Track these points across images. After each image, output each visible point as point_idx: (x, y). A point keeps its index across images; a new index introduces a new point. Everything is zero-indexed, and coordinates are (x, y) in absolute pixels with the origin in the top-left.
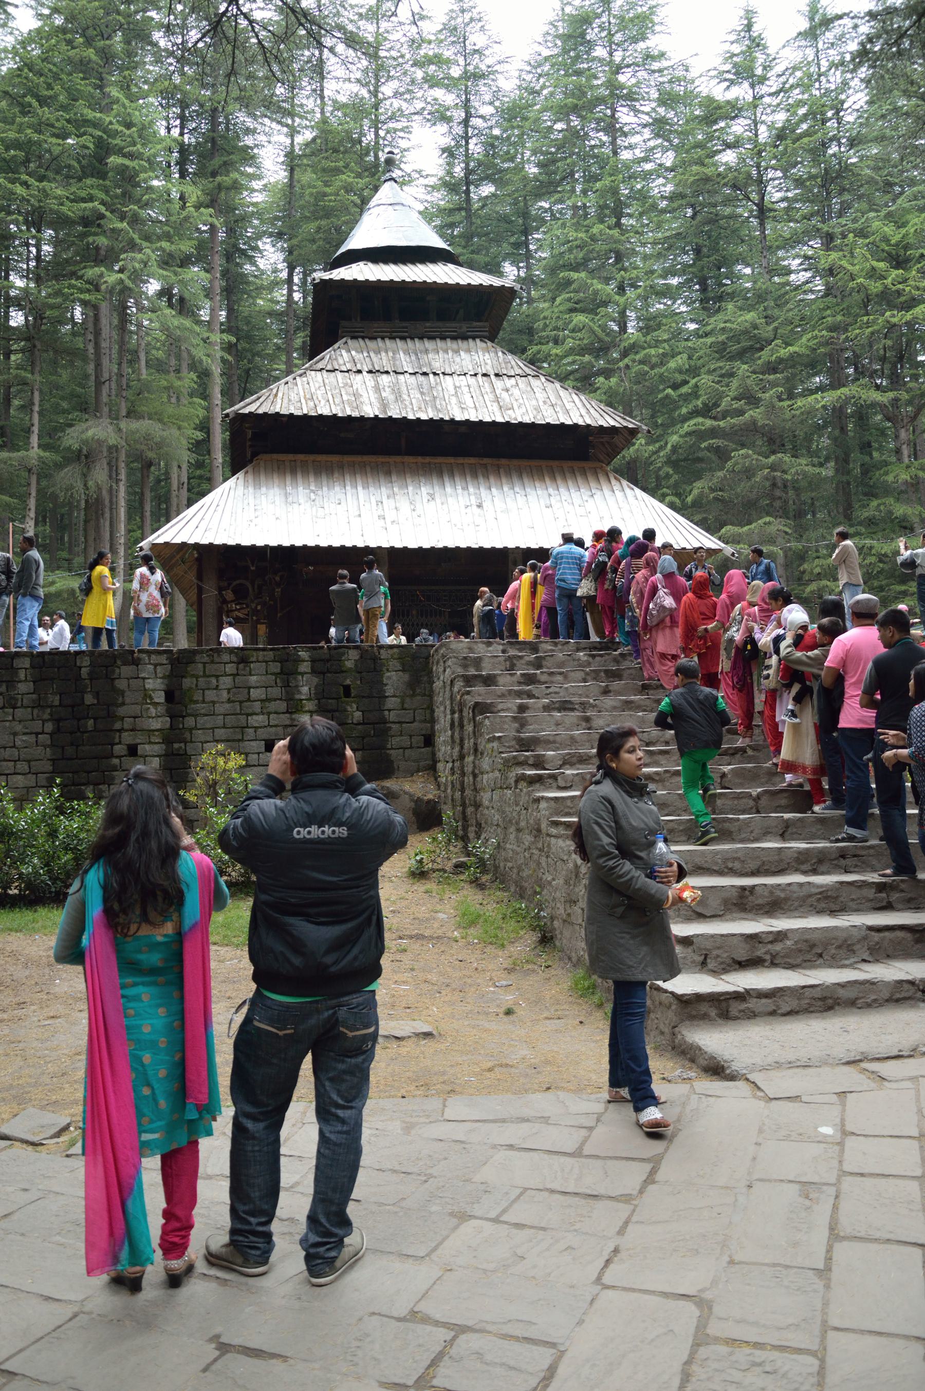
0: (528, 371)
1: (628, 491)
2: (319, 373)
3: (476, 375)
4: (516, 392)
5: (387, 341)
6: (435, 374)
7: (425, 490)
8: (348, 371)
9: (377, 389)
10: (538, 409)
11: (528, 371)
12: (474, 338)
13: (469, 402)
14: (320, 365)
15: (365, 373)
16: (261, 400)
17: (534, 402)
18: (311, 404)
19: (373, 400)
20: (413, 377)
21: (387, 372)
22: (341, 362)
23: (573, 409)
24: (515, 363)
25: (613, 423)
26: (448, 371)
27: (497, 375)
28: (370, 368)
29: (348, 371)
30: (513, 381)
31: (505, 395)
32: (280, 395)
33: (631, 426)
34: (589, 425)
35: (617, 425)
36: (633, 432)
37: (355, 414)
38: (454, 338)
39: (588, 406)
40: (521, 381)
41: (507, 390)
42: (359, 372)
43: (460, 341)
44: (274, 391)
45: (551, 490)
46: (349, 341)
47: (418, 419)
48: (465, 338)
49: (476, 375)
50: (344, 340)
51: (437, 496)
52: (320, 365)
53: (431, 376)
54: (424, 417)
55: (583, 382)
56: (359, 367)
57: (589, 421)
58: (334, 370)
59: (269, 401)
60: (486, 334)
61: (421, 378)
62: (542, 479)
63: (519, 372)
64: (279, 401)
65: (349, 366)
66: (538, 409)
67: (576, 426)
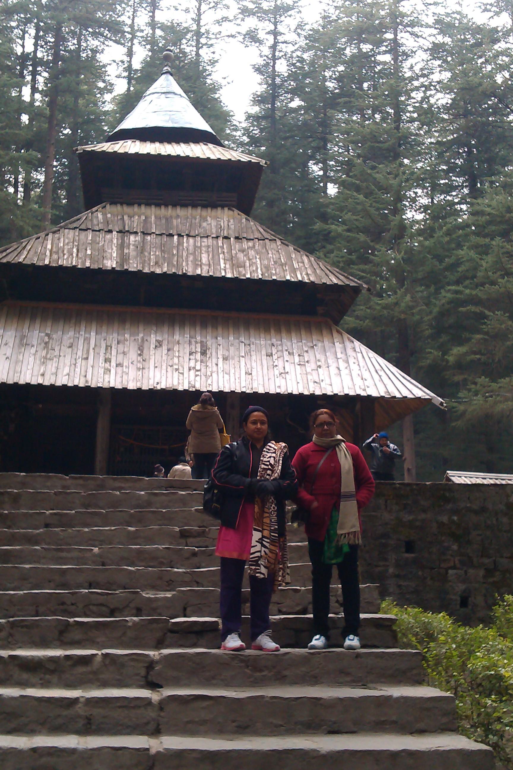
0: (266, 235)
1: (348, 343)
2: (71, 231)
3: (217, 237)
4: (252, 253)
5: (143, 207)
6: (180, 235)
7: (153, 339)
8: (99, 231)
9: (121, 247)
10: (267, 268)
11: (266, 235)
12: (223, 207)
13: (204, 260)
14: (75, 225)
15: (114, 233)
16: (8, 251)
17: (266, 262)
18: (55, 257)
19: (115, 255)
20: (159, 237)
21: (136, 233)
22: (95, 222)
23: (303, 269)
24: (254, 228)
25: (335, 281)
26: (192, 234)
27: (237, 238)
28: (121, 228)
29: (99, 231)
30: (250, 244)
31: (241, 256)
32: (28, 247)
33: (352, 284)
34: (313, 282)
35: (340, 283)
36: (356, 290)
37: (95, 266)
38: (205, 207)
39: (316, 266)
40: (258, 245)
41: (243, 251)
42: (110, 231)
43: (209, 210)
44: (24, 244)
45: (274, 341)
46: (108, 206)
47: (153, 273)
48: (214, 206)
49: (217, 237)
50: (104, 204)
51: (165, 343)
52: (75, 225)
53: (176, 237)
54: (158, 271)
55: (308, 243)
56: (110, 227)
57: (312, 279)
58: (86, 230)
59: (16, 253)
60: (234, 203)
61: (165, 238)
62: (267, 330)
63: (257, 235)
64: (25, 253)
65: (101, 226)
66: (267, 268)
67: (301, 283)
